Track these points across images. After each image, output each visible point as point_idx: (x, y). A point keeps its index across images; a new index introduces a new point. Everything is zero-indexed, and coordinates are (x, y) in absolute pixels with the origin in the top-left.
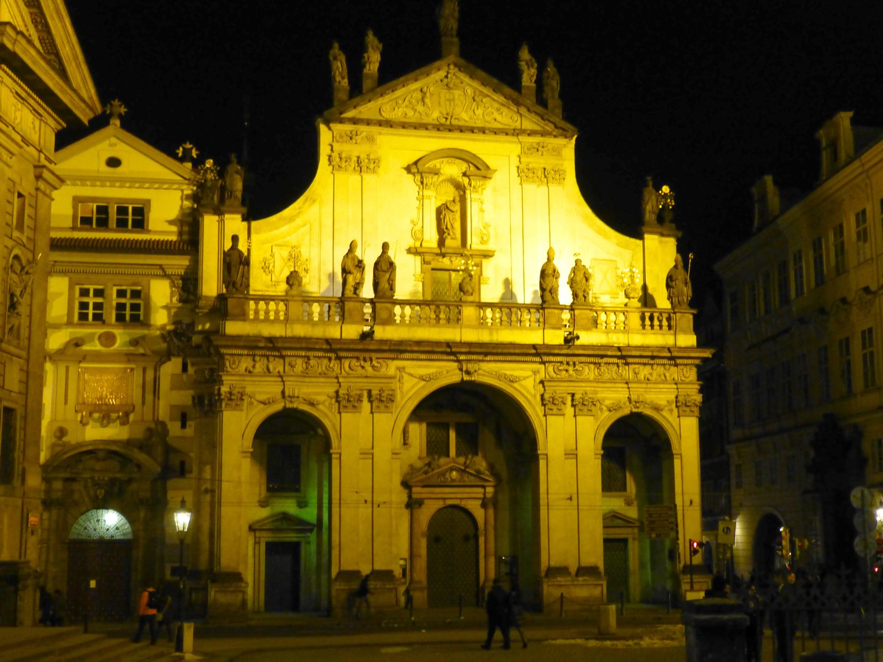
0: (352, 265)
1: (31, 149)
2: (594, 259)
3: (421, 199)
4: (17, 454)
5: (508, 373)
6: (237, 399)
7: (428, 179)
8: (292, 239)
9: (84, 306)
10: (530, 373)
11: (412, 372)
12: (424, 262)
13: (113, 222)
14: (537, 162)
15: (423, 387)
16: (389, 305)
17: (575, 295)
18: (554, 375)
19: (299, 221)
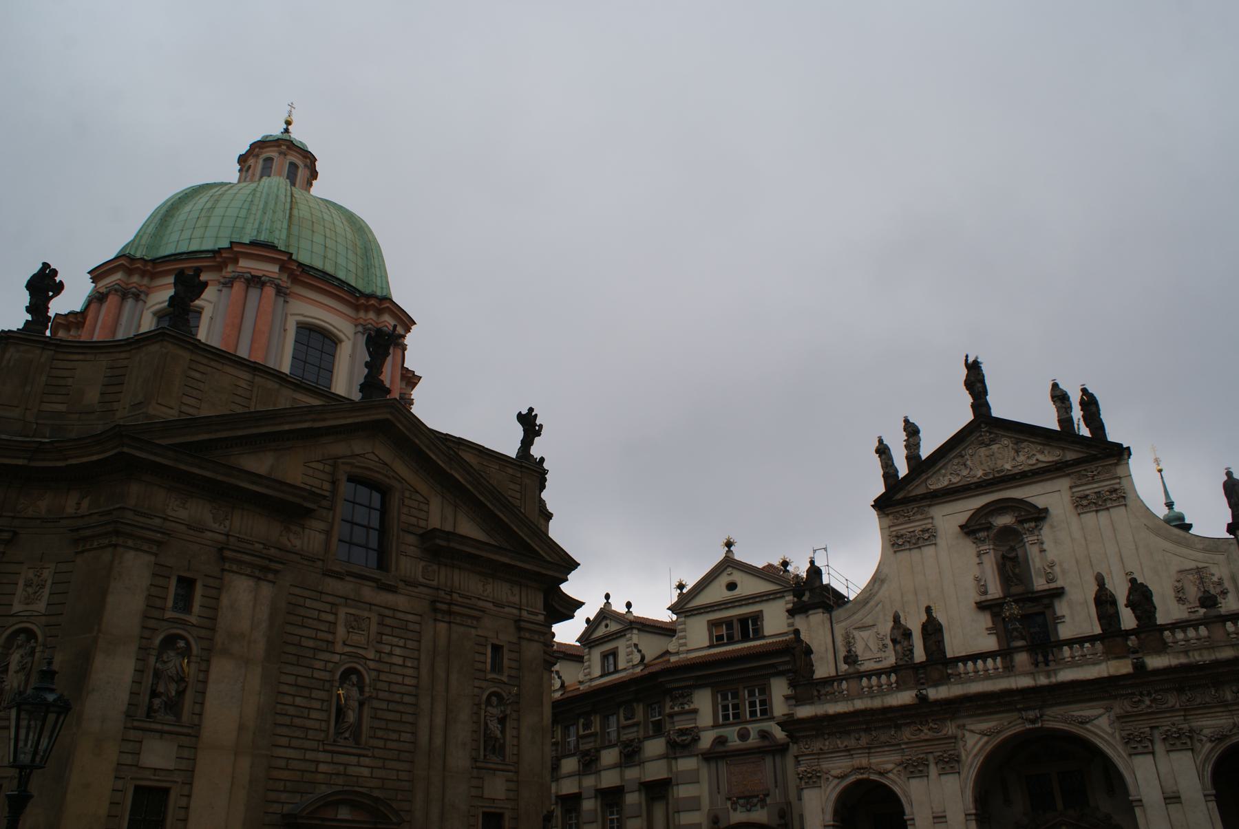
0: (901, 634)
1: (507, 610)
2: (1181, 572)
3: (979, 555)
5: (1076, 714)
6: (813, 779)
7: (982, 535)
8: (869, 620)
9: (725, 708)
10: (1101, 711)
11: (972, 727)
12: (995, 616)
14: (1090, 489)
15: (987, 743)
16: (940, 667)
17: (1137, 618)
18: (1129, 709)
19: (872, 603)
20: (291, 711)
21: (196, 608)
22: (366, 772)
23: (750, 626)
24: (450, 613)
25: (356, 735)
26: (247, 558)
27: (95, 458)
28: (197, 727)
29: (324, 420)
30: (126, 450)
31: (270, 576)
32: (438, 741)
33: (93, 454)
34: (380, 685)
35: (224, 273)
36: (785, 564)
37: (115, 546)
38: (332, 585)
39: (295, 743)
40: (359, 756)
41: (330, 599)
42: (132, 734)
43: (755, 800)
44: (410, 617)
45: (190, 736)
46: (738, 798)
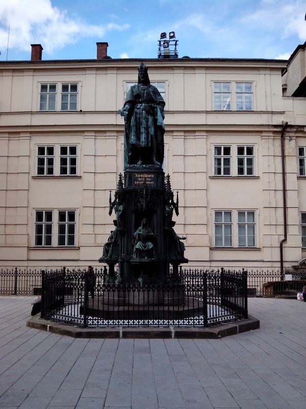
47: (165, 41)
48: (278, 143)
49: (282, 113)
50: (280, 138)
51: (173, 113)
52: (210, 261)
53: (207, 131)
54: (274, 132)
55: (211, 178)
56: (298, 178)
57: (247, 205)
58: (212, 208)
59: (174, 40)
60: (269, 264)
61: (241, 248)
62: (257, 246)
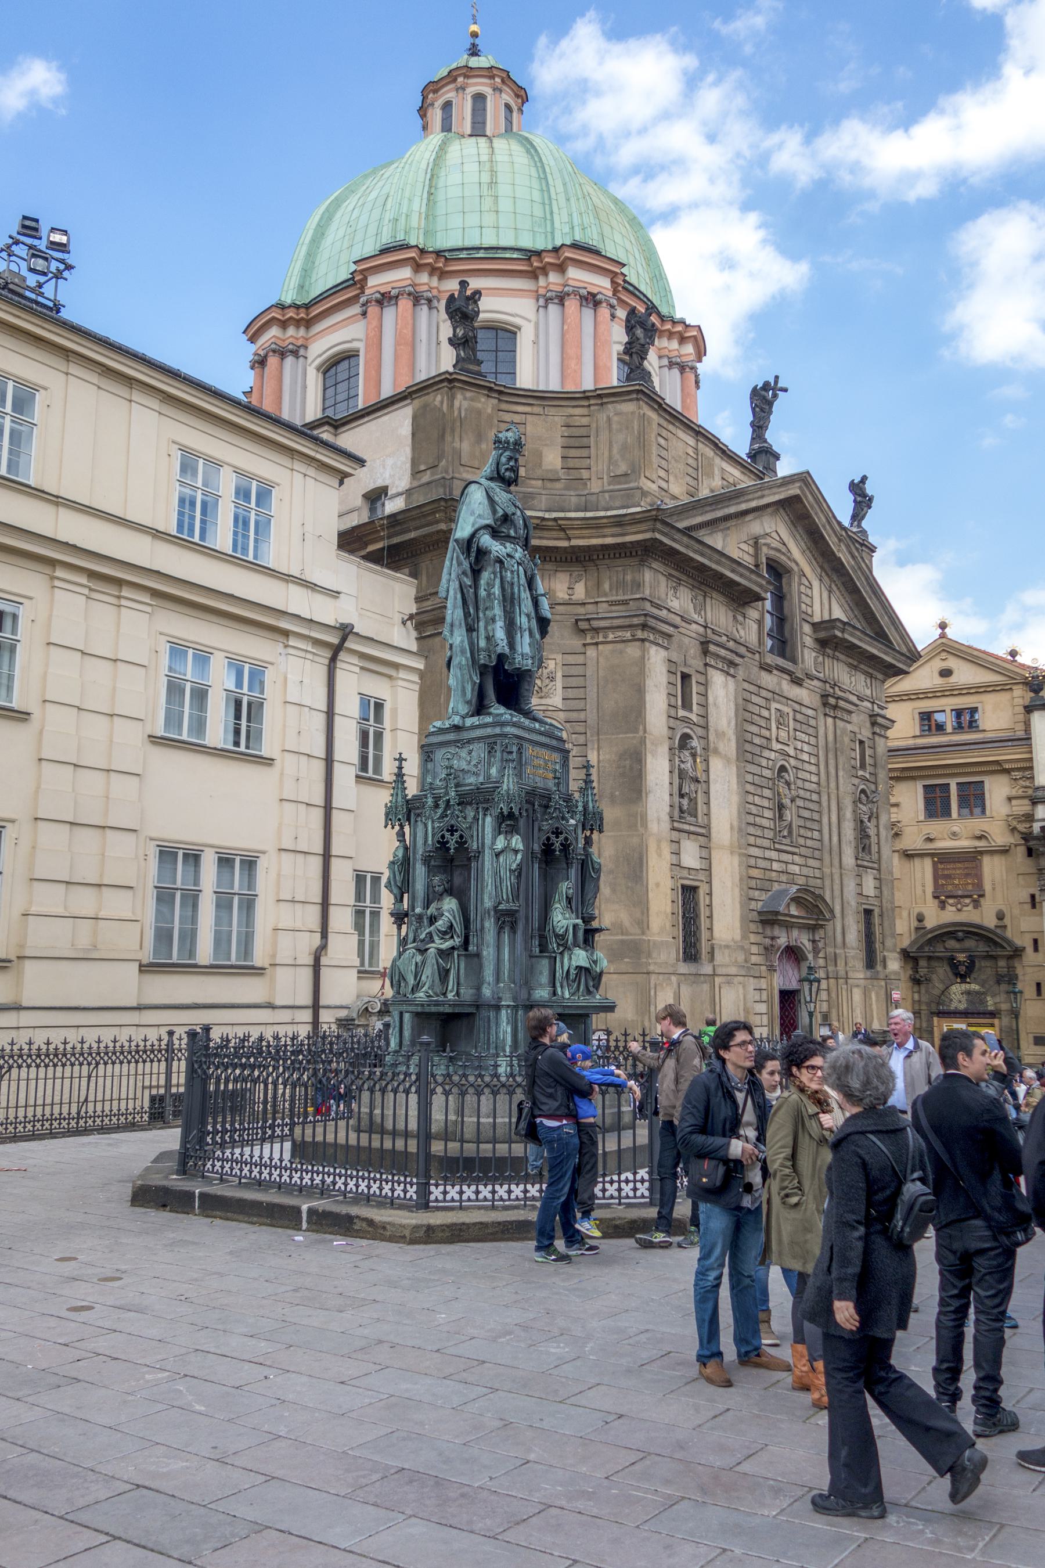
4: (878, 945)
13: (949, 729)
20: (754, 810)
21: (695, 707)
22: (796, 869)
23: (966, 719)
24: (835, 707)
25: (790, 832)
26: (723, 652)
27: (609, 541)
28: (708, 827)
29: (762, 497)
30: (658, 536)
31: (732, 671)
32: (835, 839)
33: (604, 536)
34: (800, 783)
35: (542, 282)
36: (1013, 653)
37: (643, 640)
38: (769, 680)
39: (759, 842)
40: (793, 854)
41: (764, 693)
42: (675, 835)
43: (967, 901)
44: (810, 712)
45: (704, 835)
46: (947, 897)
47: (31, 247)
48: (322, 672)
49: (335, 594)
50: (327, 662)
51: (57, 504)
52: (139, 1008)
53: (156, 593)
54: (317, 642)
55: (154, 740)
56: (357, 776)
57: (239, 840)
58: (154, 835)
59: (62, 261)
60: (285, 1016)
61: (213, 969)
62: (259, 959)
